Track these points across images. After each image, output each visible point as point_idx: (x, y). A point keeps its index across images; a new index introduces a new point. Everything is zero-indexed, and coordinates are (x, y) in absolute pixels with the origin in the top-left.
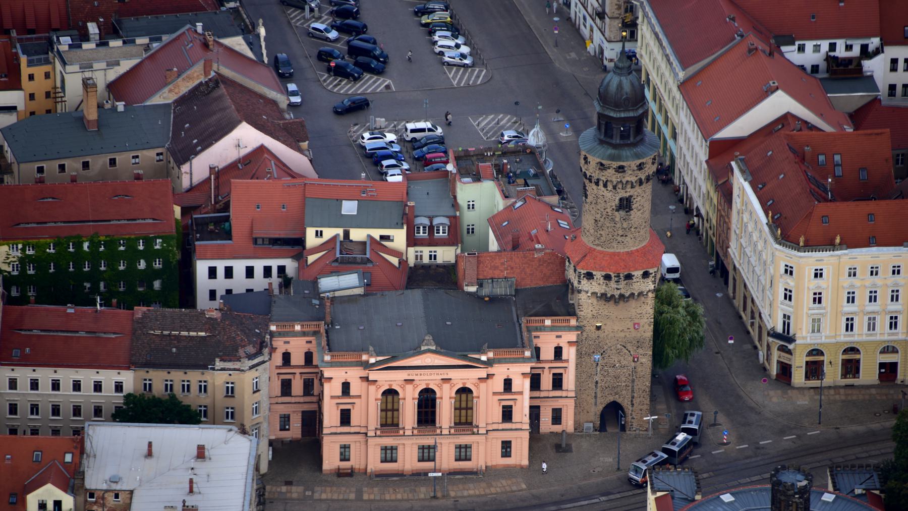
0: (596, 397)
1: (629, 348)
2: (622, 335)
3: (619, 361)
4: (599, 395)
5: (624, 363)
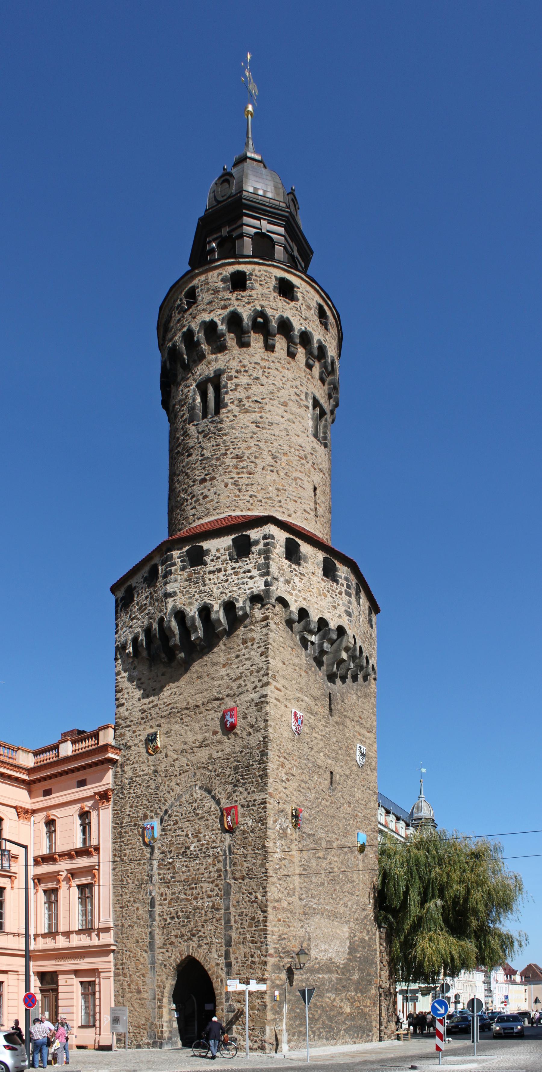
0: (152, 944)
1: (218, 791)
2: (203, 755)
3: (197, 835)
4: (159, 941)
5: (207, 836)
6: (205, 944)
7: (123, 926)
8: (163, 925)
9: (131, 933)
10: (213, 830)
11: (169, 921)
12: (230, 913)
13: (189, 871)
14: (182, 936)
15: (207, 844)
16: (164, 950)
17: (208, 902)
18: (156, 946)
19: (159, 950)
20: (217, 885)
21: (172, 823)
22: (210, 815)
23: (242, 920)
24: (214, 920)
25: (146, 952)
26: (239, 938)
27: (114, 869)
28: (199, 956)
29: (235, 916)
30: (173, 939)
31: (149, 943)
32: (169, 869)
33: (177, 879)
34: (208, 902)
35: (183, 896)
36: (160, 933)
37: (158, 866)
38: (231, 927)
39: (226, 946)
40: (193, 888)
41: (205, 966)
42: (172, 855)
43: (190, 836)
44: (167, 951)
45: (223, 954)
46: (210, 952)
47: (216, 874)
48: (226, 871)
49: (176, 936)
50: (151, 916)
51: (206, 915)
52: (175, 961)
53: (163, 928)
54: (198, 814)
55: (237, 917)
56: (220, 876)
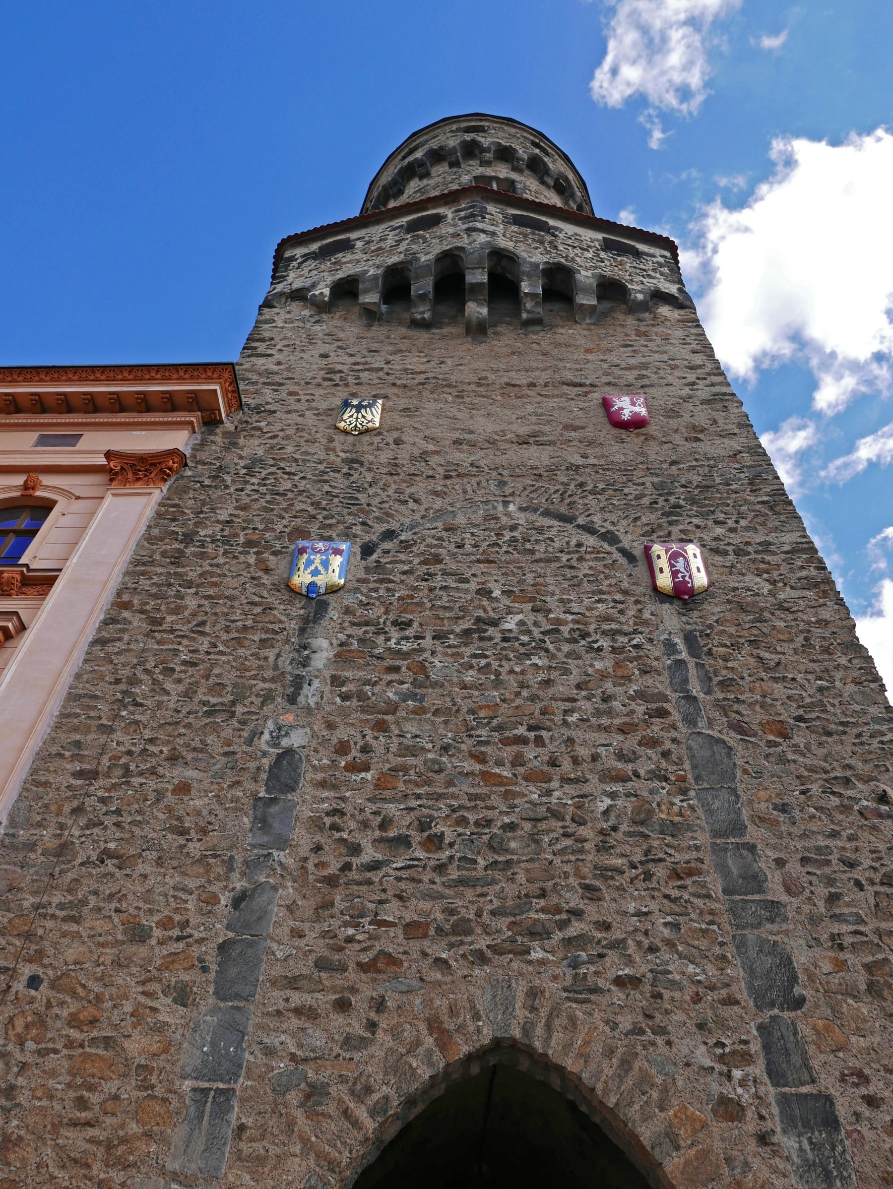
0: (236, 956)
2: (538, 456)
4: (286, 941)
6: (619, 981)
7: (63, 850)
8: (333, 868)
9: (107, 889)
10: (601, 592)
11: (370, 854)
12: (752, 848)
13: (498, 683)
14: (462, 928)
15: (575, 622)
16: (323, 1000)
17: (613, 795)
18: (266, 971)
19: (277, 995)
20: (652, 743)
21: (417, 561)
22: (580, 559)
23: (830, 881)
24: (660, 872)
25: (183, 996)
26: (841, 965)
27: (99, 642)
28: (585, 1048)
29: (780, 863)
30: (392, 942)
31: (223, 947)
32: (396, 669)
33: (433, 699)
34: (613, 795)
35: (470, 765)
36: (307, 906)
37: (338, 655)
38: (774, 909)
39: (762, 1001)
40: (521, 740)
41: (633, 1112)
42: (410, 632)
43: (496, 593)
44: (342, 1005)
45: (755, 1047)
46: (661, 1031)
47: (640, 709)
48: (691, 699)
49: (414, 930)
50: (262, 823)
51: (604, 848)
52: (396, 1066)
53: (331, 881)
54: (532, 552)
55: (794, 868)
56: (662, 713)
